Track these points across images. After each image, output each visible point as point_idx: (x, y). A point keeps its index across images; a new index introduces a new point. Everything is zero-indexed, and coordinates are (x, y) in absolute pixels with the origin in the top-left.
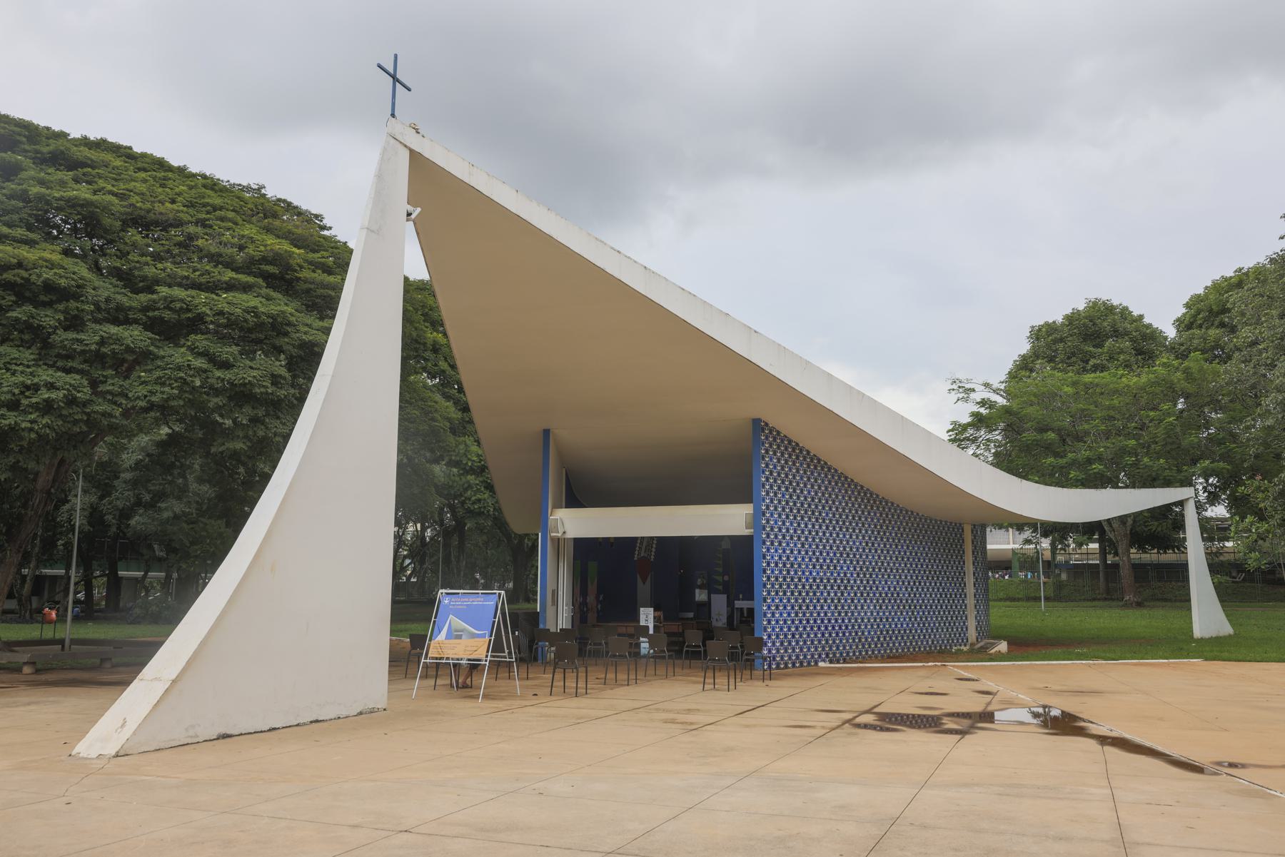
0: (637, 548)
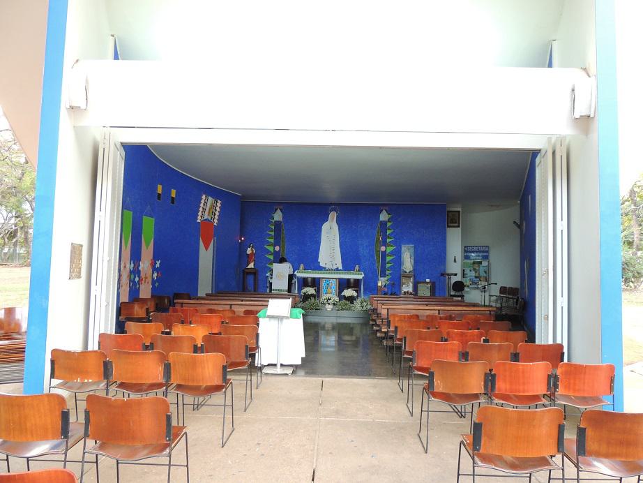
0: (201, 209)
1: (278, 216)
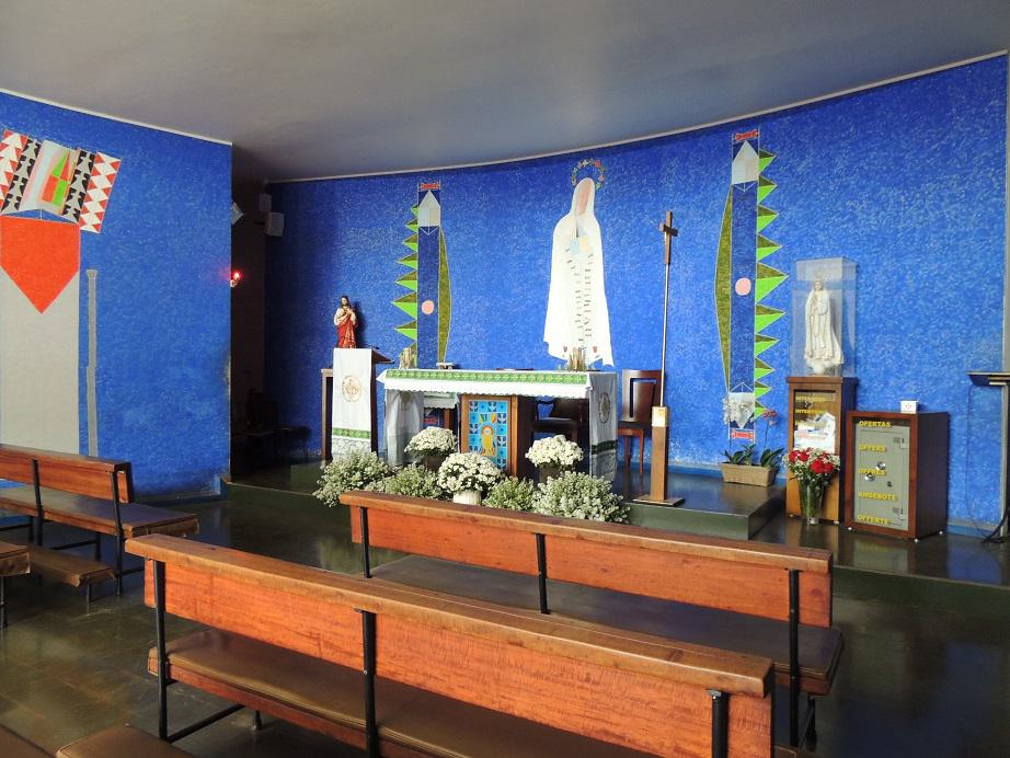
1: (428, 213)
